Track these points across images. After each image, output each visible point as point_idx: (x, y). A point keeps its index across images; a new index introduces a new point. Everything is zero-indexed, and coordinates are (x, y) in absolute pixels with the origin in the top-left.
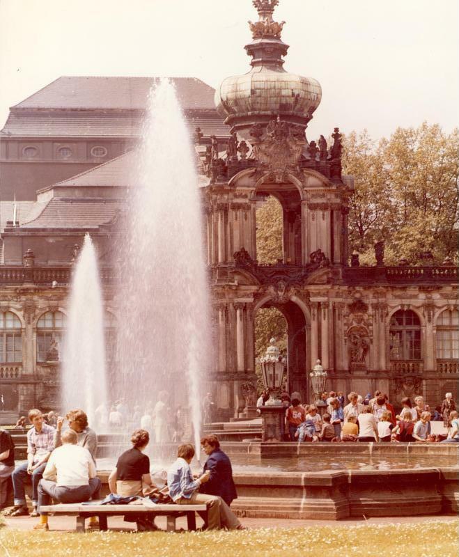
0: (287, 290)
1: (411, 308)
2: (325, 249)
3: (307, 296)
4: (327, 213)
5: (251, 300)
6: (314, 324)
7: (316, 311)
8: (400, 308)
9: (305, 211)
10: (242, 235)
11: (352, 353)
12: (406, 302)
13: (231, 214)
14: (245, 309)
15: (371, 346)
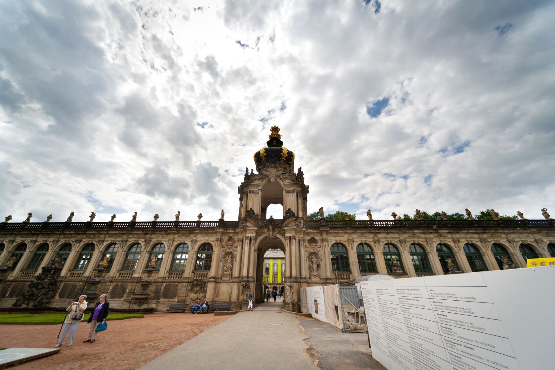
0: (274, 231)
1: (341, 242)
2: (294, 210)
3: (283, 235)
4: (295, 194)
5: (254, 235)
6: (287, 249)
7: (288, 241)
8: (335, 242)
9: (284, 193)
10: (253, 204)
11: (310, 268)
12: (338, 239)
13: (249, 195)
14: (250, 241)
15: (321, 263)
